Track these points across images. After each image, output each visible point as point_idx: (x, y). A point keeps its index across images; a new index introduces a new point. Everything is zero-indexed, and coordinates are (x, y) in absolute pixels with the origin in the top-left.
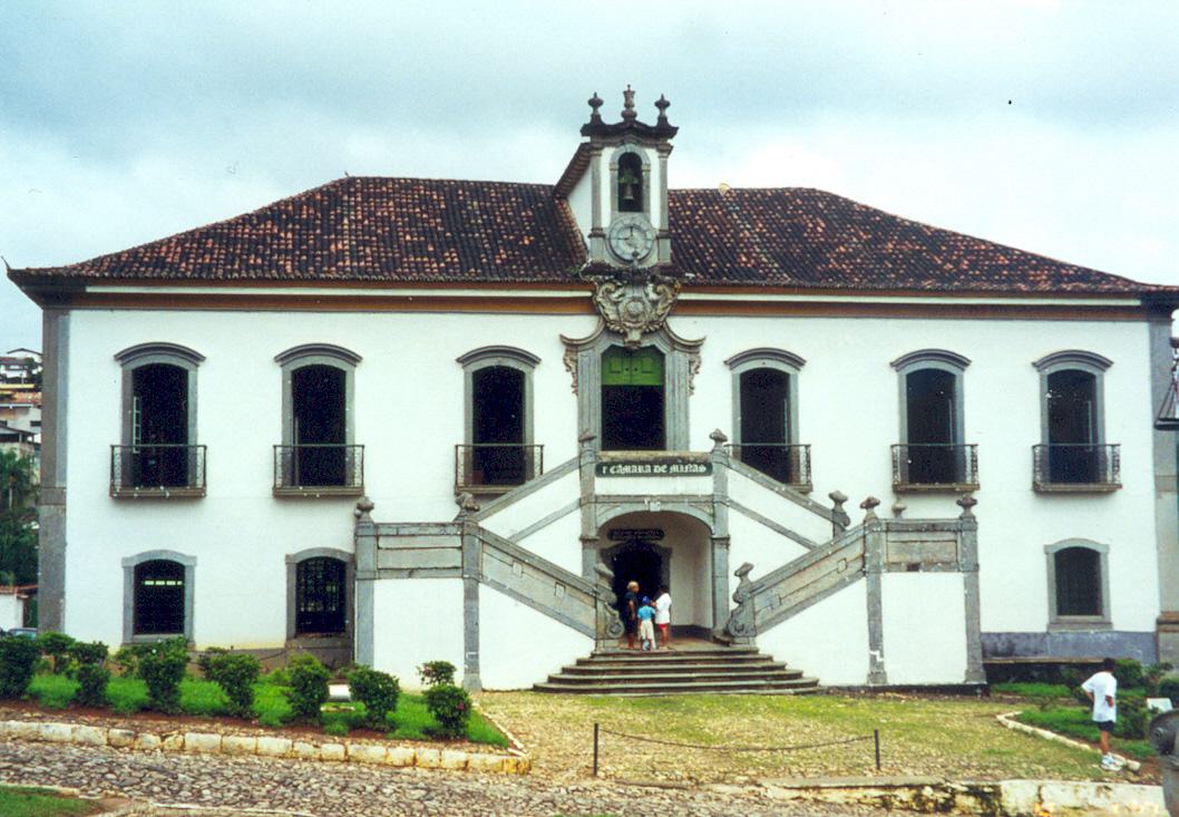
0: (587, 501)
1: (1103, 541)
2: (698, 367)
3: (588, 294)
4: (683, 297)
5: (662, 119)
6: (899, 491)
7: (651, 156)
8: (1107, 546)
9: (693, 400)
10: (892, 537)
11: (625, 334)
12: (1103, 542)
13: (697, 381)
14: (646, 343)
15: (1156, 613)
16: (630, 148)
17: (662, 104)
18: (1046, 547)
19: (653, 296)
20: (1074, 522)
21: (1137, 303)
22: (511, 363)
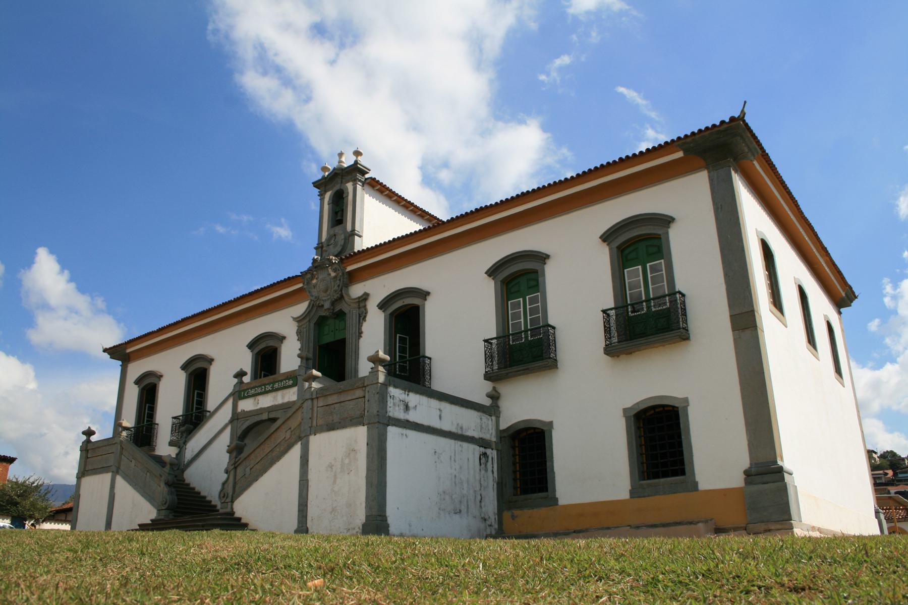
0: (236, 417)
1: (679, 394)
2: (365, 317)
3: (301, 285)
4: (349, 269)
5: (356, 162)
6: (488, 377)
7: (350, 186)
8: (686, 400)
9: (361, 340)
10: (321, 402)
11: (323, 306)
12: (680, 396)
13: (365, 327)
14: (337, 309)
15: (745, 463)
16: (337, 187)
17: (357, 153)
18: (625, 410)
19: (333, 274)
20: (654, 377)
21: (680, 154)
22: (272, 343)
